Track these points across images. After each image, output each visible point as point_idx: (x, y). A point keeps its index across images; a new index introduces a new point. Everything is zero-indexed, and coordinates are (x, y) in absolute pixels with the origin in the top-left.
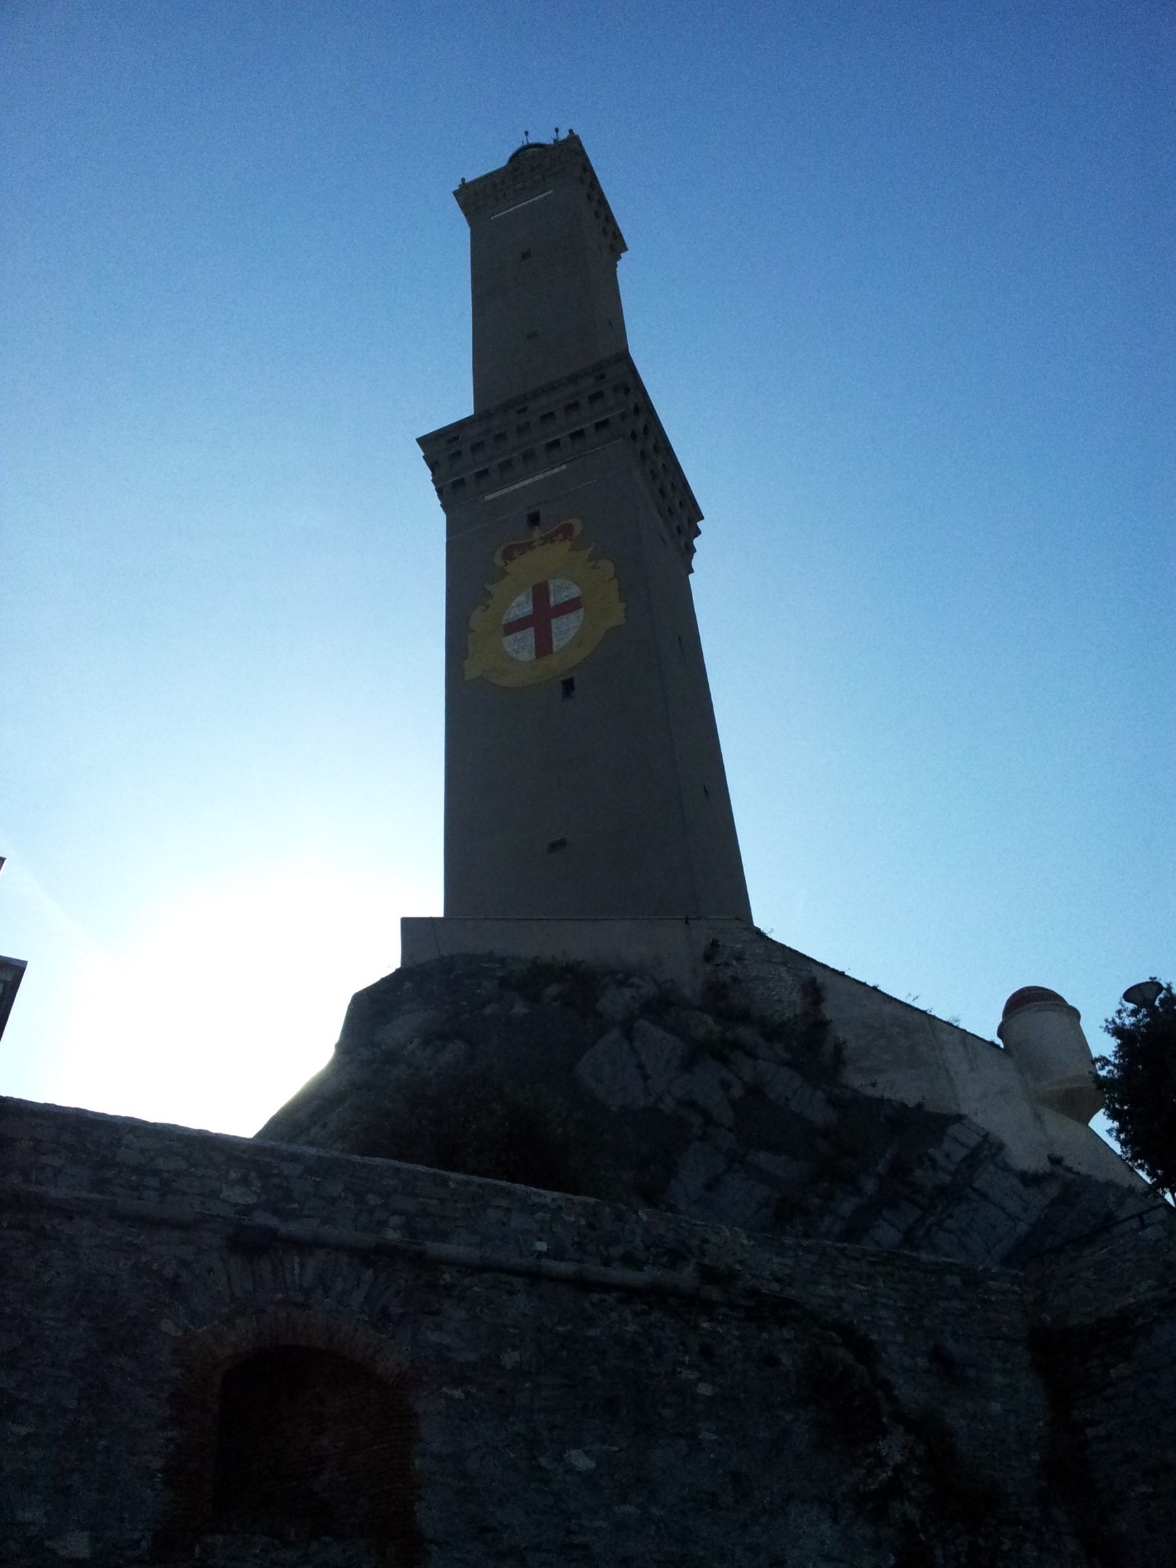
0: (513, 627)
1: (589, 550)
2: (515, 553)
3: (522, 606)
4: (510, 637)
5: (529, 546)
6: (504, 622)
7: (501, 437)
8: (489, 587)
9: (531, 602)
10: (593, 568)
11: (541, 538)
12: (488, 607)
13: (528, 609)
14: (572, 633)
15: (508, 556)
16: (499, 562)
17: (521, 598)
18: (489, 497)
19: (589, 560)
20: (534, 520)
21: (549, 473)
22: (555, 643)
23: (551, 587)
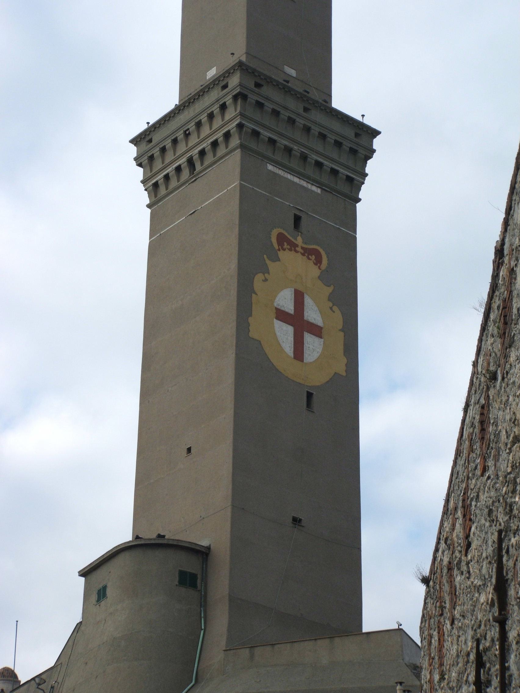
0: (282, 315)
2: (286, 246)
3: (285, 300)
4: (279, 322)
6: (275, 305)
7: (291, 121)
8: (268, 262)
9: (293, 301)
10: (331, 308)
11: (302, 248)
12: (266, 280)
13: (289, 307)
14: (316, 355)
16: (274, 241)
18: (270, 167)
19: (329, 300)
21: (309, 186)
22: (306, 356)
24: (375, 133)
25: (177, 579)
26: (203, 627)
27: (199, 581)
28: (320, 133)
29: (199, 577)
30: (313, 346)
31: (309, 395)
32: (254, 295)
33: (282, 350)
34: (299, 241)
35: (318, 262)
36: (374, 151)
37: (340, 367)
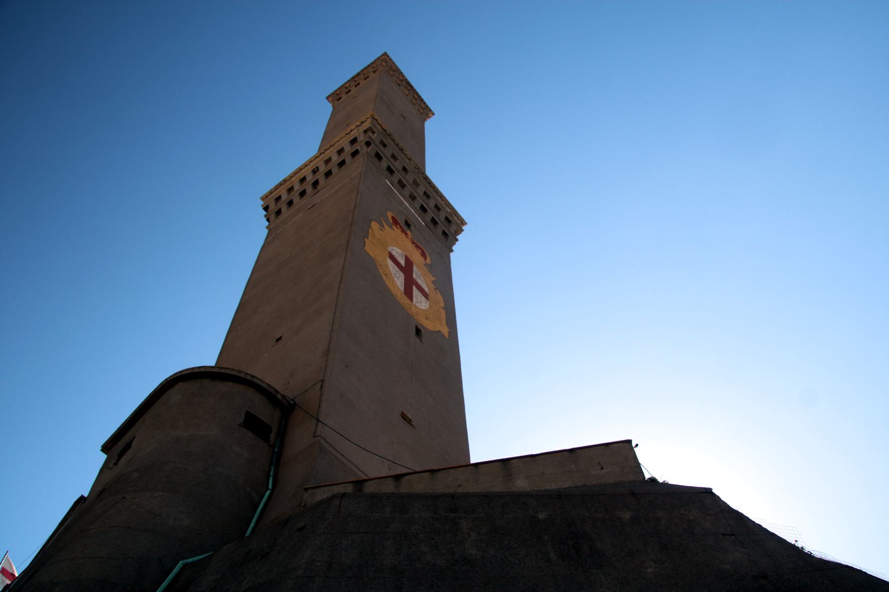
1: (434, 279)
5: (406, 234)
13: (402, 262)
14: (423, 308)
15: (395, 222)
17: (400, 251)
19: (433, 282)
20: (408, 224)
23: (415, 268)
24: (463, 223)
25: (242, 419)
26: (270, 487)
27: (272, 436)
28: (425, 193)
29: (274, 431)
30: (420, 302)
31: (418, 332)
32: (370, 231)
33: (393, 281)
34: (409, 232)
35: (423, 255)
36: (462, 230)
37: (445, 331)
